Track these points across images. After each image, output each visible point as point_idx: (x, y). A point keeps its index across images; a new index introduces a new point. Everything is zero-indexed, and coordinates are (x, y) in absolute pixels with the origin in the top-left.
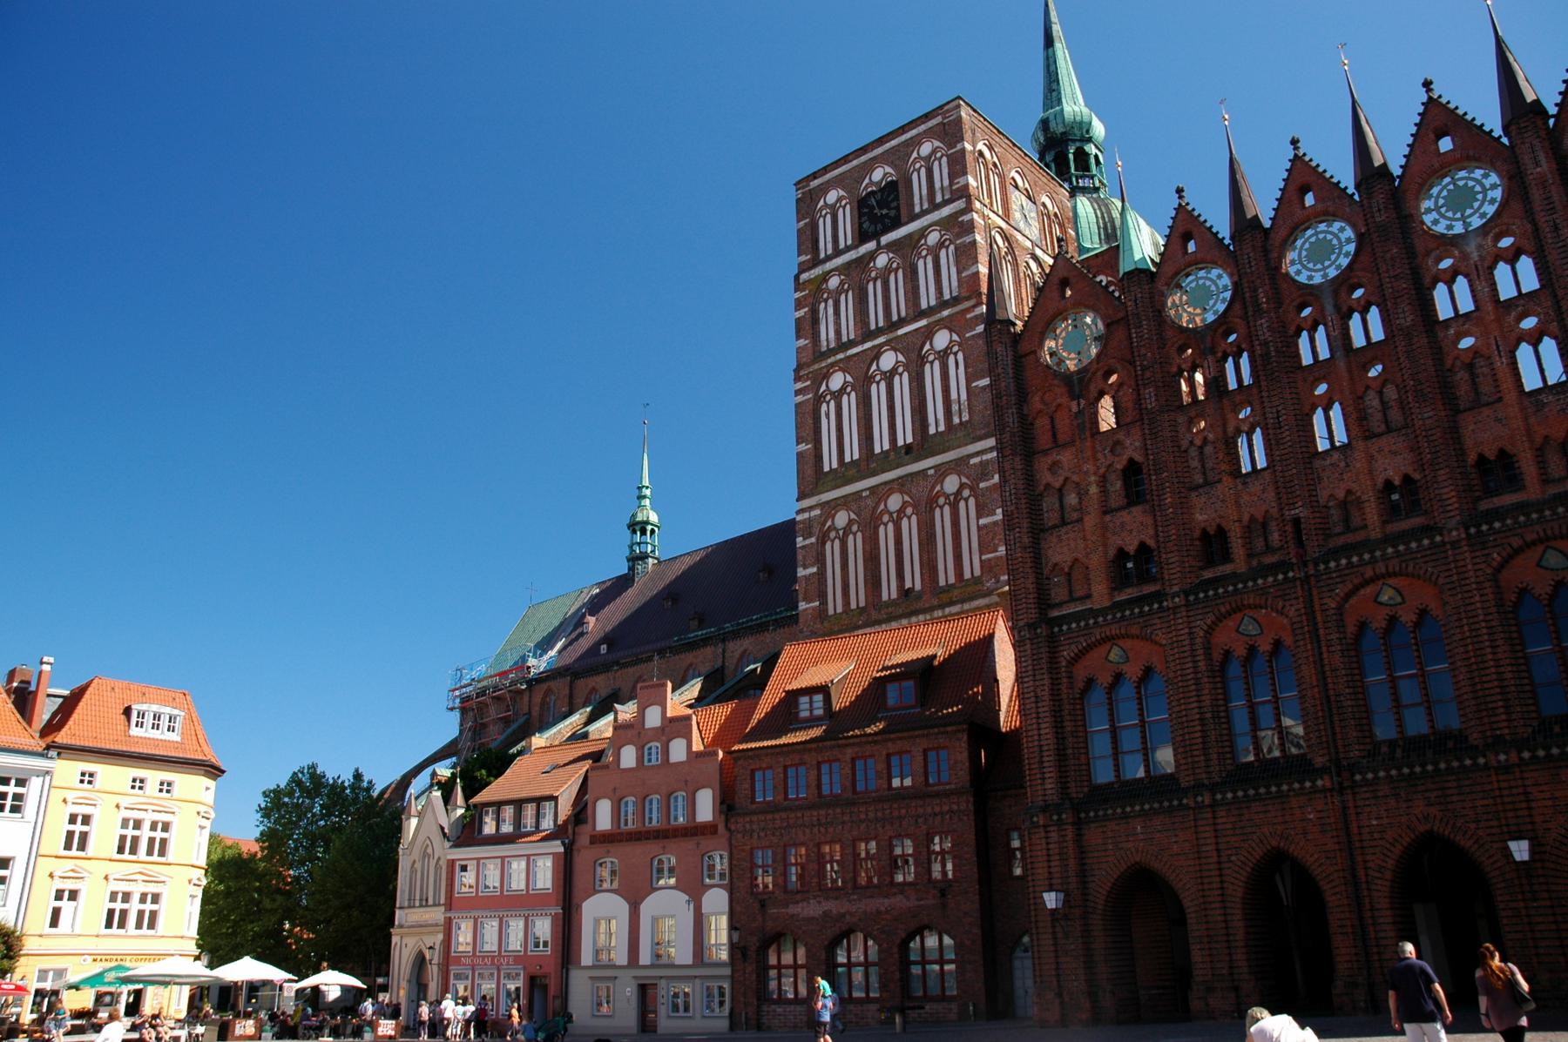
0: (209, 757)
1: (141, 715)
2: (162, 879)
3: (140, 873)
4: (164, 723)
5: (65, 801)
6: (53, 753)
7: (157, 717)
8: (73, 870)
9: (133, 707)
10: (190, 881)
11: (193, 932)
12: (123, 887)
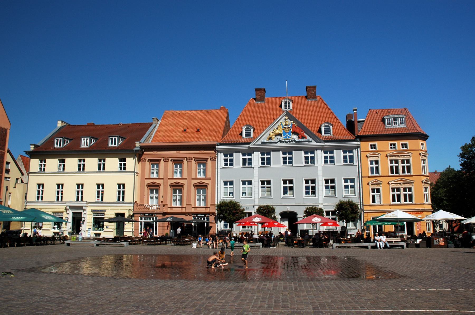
0: (419, 131)
1: (389, 119)
2: (411, 182)
3: (401, 180)
4: (399, 121)
5: (367, 156)
6: (358, 139)
7: (395, 119)
8: (375, 182)
9: (385, 117)
10: (422, 182)
11: (429, 202)
12: (395, 186)
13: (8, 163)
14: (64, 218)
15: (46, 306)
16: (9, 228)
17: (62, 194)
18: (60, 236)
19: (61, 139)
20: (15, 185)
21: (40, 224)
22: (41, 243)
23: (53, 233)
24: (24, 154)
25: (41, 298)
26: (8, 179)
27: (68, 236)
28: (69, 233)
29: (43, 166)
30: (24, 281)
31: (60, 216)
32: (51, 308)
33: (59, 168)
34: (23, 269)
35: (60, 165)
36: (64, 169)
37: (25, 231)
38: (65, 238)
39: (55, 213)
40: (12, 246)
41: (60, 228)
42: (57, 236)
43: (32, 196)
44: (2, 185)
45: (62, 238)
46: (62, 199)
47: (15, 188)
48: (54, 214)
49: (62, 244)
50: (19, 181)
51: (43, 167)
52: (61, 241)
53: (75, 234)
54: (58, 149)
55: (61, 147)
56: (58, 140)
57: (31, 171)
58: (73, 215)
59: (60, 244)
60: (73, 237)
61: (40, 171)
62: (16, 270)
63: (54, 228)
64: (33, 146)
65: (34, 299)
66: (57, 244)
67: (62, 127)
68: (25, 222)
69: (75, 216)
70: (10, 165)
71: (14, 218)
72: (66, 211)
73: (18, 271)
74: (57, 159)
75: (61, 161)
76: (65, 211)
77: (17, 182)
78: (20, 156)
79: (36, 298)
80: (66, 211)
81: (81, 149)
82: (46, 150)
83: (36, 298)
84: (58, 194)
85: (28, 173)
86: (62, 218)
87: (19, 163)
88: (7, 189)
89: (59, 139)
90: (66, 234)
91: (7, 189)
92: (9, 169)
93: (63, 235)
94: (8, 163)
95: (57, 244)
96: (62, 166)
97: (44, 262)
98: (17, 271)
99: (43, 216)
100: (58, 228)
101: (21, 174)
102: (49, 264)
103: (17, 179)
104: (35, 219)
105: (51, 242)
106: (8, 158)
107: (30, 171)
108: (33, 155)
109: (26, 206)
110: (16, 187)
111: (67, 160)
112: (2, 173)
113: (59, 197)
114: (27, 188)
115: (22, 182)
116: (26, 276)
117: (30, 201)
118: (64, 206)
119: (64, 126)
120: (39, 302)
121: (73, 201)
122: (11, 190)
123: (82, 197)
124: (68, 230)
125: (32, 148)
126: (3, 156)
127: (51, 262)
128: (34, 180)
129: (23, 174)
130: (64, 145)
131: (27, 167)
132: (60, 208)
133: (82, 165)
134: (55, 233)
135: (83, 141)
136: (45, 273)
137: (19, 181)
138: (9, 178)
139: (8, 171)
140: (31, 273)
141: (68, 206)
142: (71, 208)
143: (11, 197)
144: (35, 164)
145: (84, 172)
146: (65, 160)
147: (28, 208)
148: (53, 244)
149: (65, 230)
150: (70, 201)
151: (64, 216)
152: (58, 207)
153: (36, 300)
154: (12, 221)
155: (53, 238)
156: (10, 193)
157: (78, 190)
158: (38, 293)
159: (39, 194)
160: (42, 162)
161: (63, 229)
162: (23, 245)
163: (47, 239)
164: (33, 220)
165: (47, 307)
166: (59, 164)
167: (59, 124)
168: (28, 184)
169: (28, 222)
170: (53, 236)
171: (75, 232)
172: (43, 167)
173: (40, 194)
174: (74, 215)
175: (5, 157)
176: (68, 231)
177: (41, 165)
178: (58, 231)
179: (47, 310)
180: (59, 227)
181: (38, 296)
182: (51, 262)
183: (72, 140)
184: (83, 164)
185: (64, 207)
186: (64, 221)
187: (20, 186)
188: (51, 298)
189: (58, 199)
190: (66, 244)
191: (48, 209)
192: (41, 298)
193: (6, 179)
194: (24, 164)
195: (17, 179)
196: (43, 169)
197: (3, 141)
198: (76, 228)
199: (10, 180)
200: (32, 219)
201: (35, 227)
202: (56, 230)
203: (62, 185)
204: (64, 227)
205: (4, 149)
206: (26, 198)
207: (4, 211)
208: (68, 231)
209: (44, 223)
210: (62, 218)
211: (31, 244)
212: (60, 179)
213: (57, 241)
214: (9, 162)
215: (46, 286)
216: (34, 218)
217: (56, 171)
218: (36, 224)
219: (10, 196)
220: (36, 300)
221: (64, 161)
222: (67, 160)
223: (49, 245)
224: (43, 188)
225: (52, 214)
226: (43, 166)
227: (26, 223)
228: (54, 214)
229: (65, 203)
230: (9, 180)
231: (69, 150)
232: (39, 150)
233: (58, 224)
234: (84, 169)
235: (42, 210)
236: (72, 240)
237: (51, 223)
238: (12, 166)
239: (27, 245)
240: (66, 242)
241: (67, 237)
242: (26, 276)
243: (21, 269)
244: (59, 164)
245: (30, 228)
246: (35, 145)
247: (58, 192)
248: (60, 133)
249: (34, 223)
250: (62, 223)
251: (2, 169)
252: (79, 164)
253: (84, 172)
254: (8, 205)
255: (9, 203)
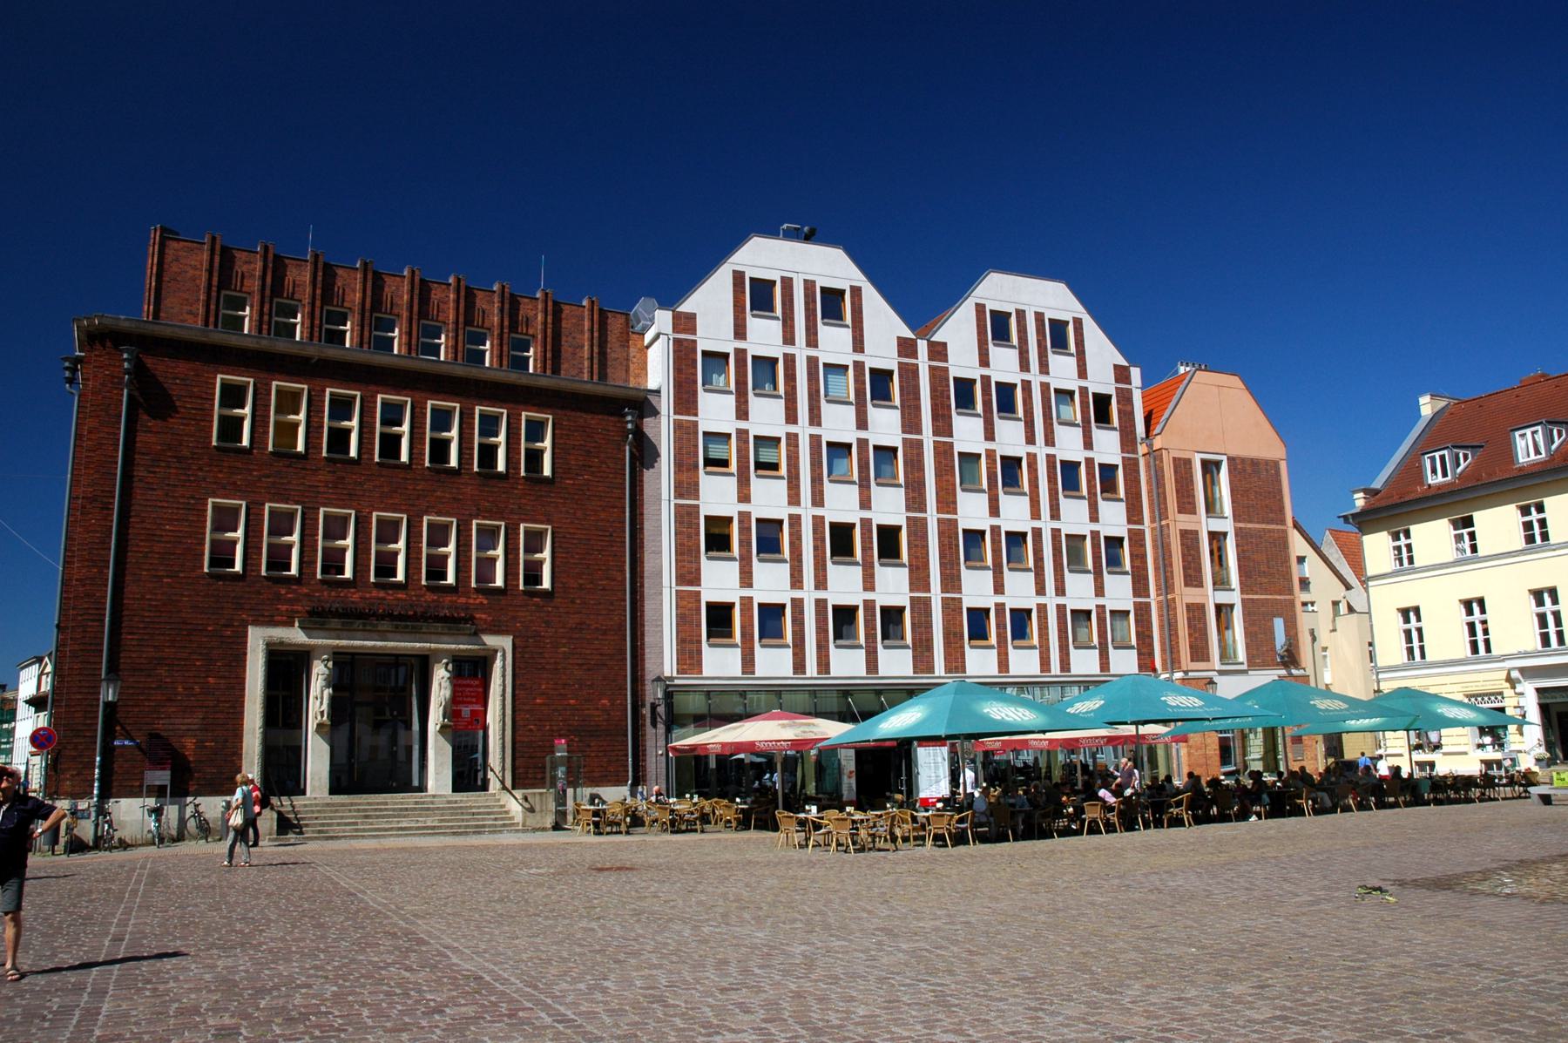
13: (1301, 560)
14: (1509, 712)
15: (1532, 1008)
16: (1342, 755)
17: (1486, 632)
18: (1507, 771)
19: (1441, 453)
20: (1334, 620)
21: (1433, 737)
22: (1449, 796)
23: (1482, 761)
24: (1340, 525)
25: (1503, 977)
26: (1310, 608)
27: (1536, 769)
28: (1538, 760)
29: (1404, 550)
30: (1430, 916)
31: (1494, 705)
32: (1549, 1019)
33: (1457, 549)
34: (1414, 877)
35: (1459, 538)
36: (1474, 549)
37: (1395, 762)
38: (1528, 779)
39: (1476, 696)
40: (1362, 807)
41: (1501, 746)
42: (1495, 772)
43: (1391, 649)
44: (1300, 629)
45: (1515, 779)
46: (1488, 649)
47: (1334, 630)
48: (1473, 700)
49: (1519, 797)
50: (1343, 608)
51: (1405, 554)
52: (1517, 788)
53: (1562, 763)
54: (1440, 487)
55: (1449, 478)
56: (1433, 459)
57: (1370, 573)
58: (1539, 698)
59: (1513, 798)
60: (1558, 773)
61: (1398, 567)
62: (1395, 881)
63: (1481, 746)
64: (1362, 495)
65: (1477, 978)
66: (1503, 799)
67: (1436, 415)
68: (1384, 731)
69: (1548, 701)
70: (1306, 564)
71: (1353, 722)
72: (1513, 687)
73: (1402, 884)
74: (1446, 520)
75: (1460, 524)
76: (1508, 685)
77: (1336, 613)
78: (1328, 532)
79: (1482, 975)
80: (1513, 687)
81: (1521, 469)
82: (1403, 500)
83: (1486, 978)
84: (1472, 631)
85: (1365, 581)
86: (1502, 710)
87: (1332, 554)
88: (1314, 639)
89: (1437, 455)
90: (1527, 763)
91: (1314, 639)
92: (1307, 576)
93: (1517, 768)
94: (1301, 560)
95: (1503, 799)
96: (1466, 538)
97: (1477, 859)
98: (1400, 885)
99: (1439, 711)
100: (1493, 744)
101: (1344, 588)
102: (1495, 865)
103: (1336, 604)
104: (1415, 720)
105: (1483, 794)
106: (1298, 545)
107: (1370, 573)
108: (1367, 521)
109: (1378, 682)
110: (1338, 628)
111: (1478, 516)
112: (1290, 591)
113: (1479, 641)
114: (1371, 626)
115: (1351, 609)
116: (1431, 901)
117: (1389, 667)
118: (1501, 669)
119: (1443, 408)
120: (1498, 990)
121: (1529, 649)
122: (1324, 637)
123: (1562, 631)
124: (1532, 749)
125: (1360, 501)
126: (1282, 543)
127: (1500, 860)
128: (1386, 600)
129: (1348, 587)
130: (1459, 470)
131: (1356, 559)
132: (1488, 678)
133: (1536, 526)
134: (1488, 764)
135: (1520, 444)
136: (1488, 895)
137: (1343, 608)
138: (1313, 604)
139: (1305, 584)
140: (1444, 892)
141: (1514, 668)
142: (1528, 673)
143: (1328, 659)
144: (1378, 547)
145: (1549, 545)
146: (1471, 517)
147: (1386, 687)
148: (1490, 799)
149: (1520, 752)
150: (1520, 653)
151: (1509, 703)
152: (1481, 677)
153: (1487, 981)
154: (1347, 732)
155: (1487, 781)
156: (1325, 649)
157: (1541, 610)
158: (1488, 962)
159: (1409, 639)
160: (1399, 539)
161: (1514, 747)
162: (1395, 805)
163: (1468, 782)
164: (1411, 724)
165: (1533, 1013)
166: (1456, 536)
167: (1427, 407)
168: (1369, 613)
169: (1395, 731)
170: (1486, 773)
171: (1561, 756)
172: (1405, 554)
173: (1414, 642)
174: (1545, 698)
175: (1291, 545)
176: (1533, 753)
177: (1398, 549)
178: (1498, 756)
179: (1537, 1022)
180: (1499, 743)
181: (1486, 969)
182: (1500, 860)
183: (1482, 447)
184: (1539, 521)
185: (1504, 675)
186: (1512, 720)
187: (1347, 623)
188: (1537, 982)
189: (1475, 649)
190: (1535, 799)
191: (1450, 685)
192: (1503, 977)
193: (1305, 608)
194: (1346, 556)
195: (1336, 604)
196: (1405, 561)
197: (1275, 497)
198: (1559, 743)
199: (1315, 608)
200: (1407, 721)
201: (1418, 747)
202: (1491, 754)
203: (1481, 602)
204: (1512, 736)
205: (1283, 521)
206: (1372, 657)
207: (1322, 704)
208: (1533, 753)
209: (1444, 732)
210: (1502, 710)
211: (1418, 801)
212: (1471, 582)
213: (1501, 788)
214: (1303, 555)
215: (1505, 938)
216: (1410, 719)
217: (1451, 560)
218: (1418, 736)
219: (1325, 657)
220: (1487, 981)
221: (1468, 522)
222: (1478, 516)
223: (1478, 804)
224: (1419, 620)
225: (1466, 700)
226: (1404, 550)
227: (1389, 734)
228: (1473, 700)
229: (1503, 660)
230: (1313, 611)
231: (1479, 483)
232: (1384, 504)
233: (1494, 731)
234: (1545, 537)
235: (1432, 691)
236: (1555, 785)
237: (1468, 729)
238: (1313, 568)
239: (1407, 804)
240: (1533, 790)
241: (1535, 773)
242: (1431, 901)
243: (1409, 879)
244: (1456, 536)
245: (1405, 751)
246: (1365, 491)
247: (1471, 626)
248: (1439, 434)
249: (1412, 733)
250: (1505, 728)
251: (1290, 580)
252: (1524, 523)
253: (1549, 545)
254: (1327, 685)
255: (1328, 677)
